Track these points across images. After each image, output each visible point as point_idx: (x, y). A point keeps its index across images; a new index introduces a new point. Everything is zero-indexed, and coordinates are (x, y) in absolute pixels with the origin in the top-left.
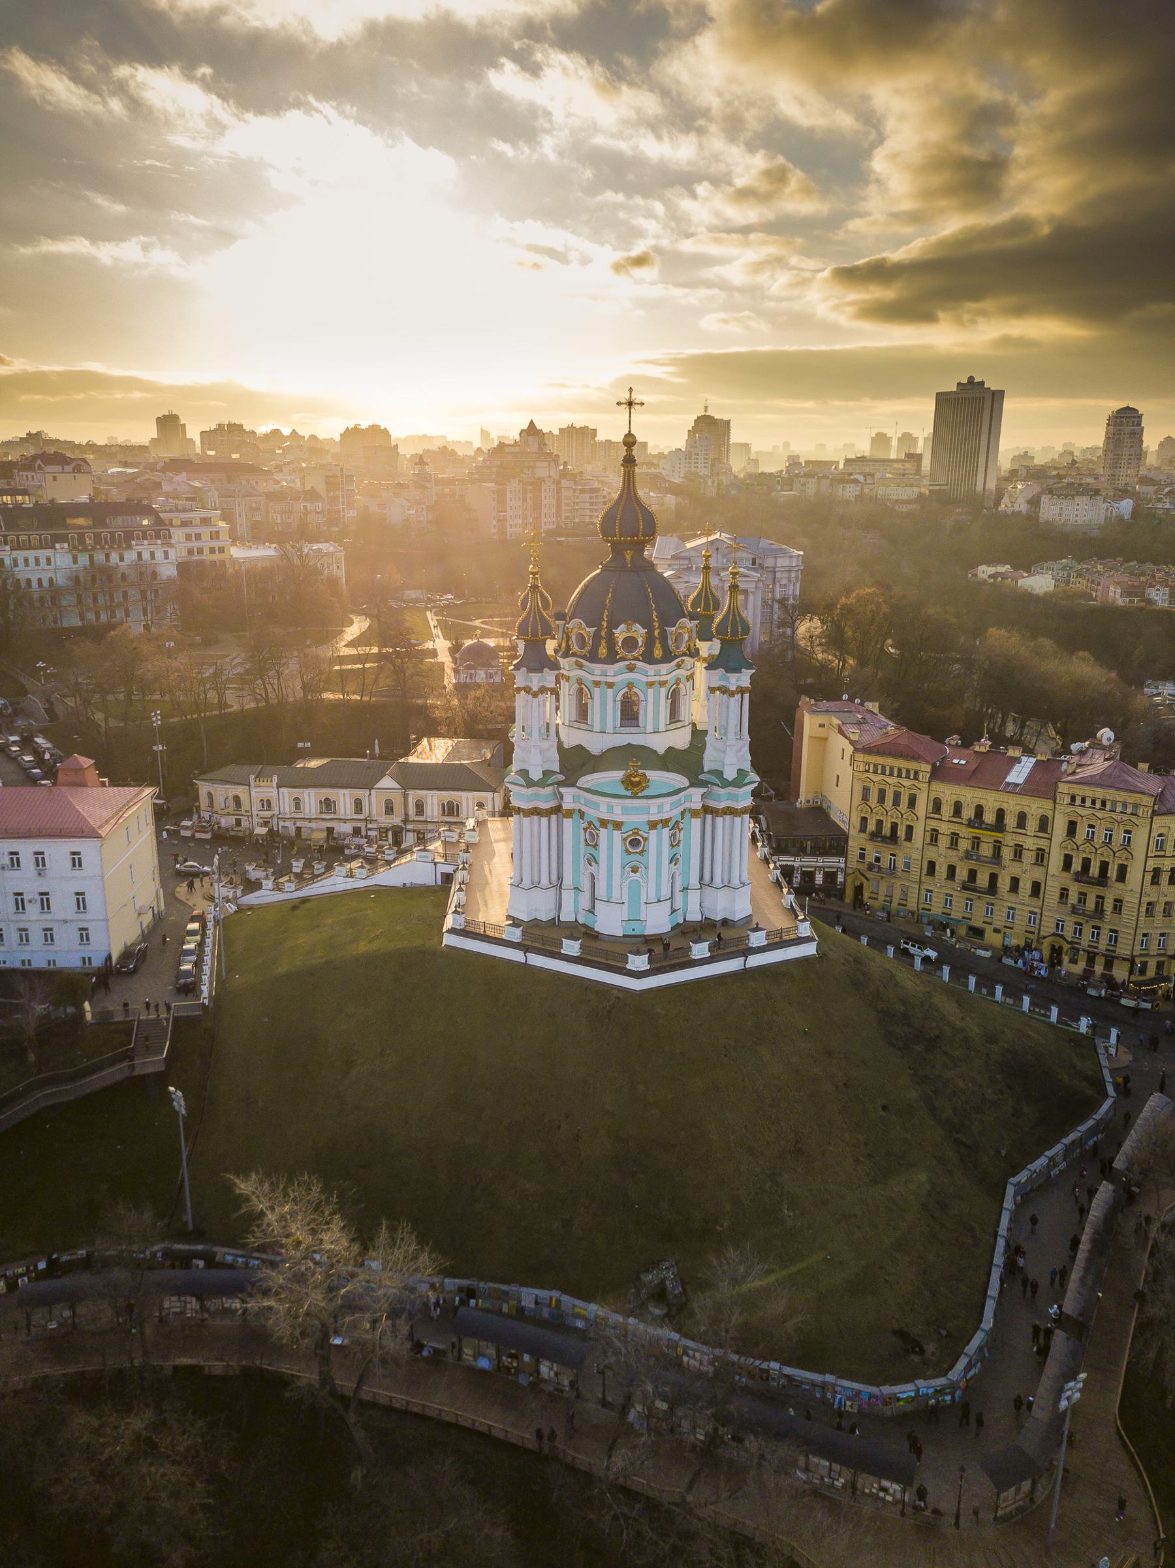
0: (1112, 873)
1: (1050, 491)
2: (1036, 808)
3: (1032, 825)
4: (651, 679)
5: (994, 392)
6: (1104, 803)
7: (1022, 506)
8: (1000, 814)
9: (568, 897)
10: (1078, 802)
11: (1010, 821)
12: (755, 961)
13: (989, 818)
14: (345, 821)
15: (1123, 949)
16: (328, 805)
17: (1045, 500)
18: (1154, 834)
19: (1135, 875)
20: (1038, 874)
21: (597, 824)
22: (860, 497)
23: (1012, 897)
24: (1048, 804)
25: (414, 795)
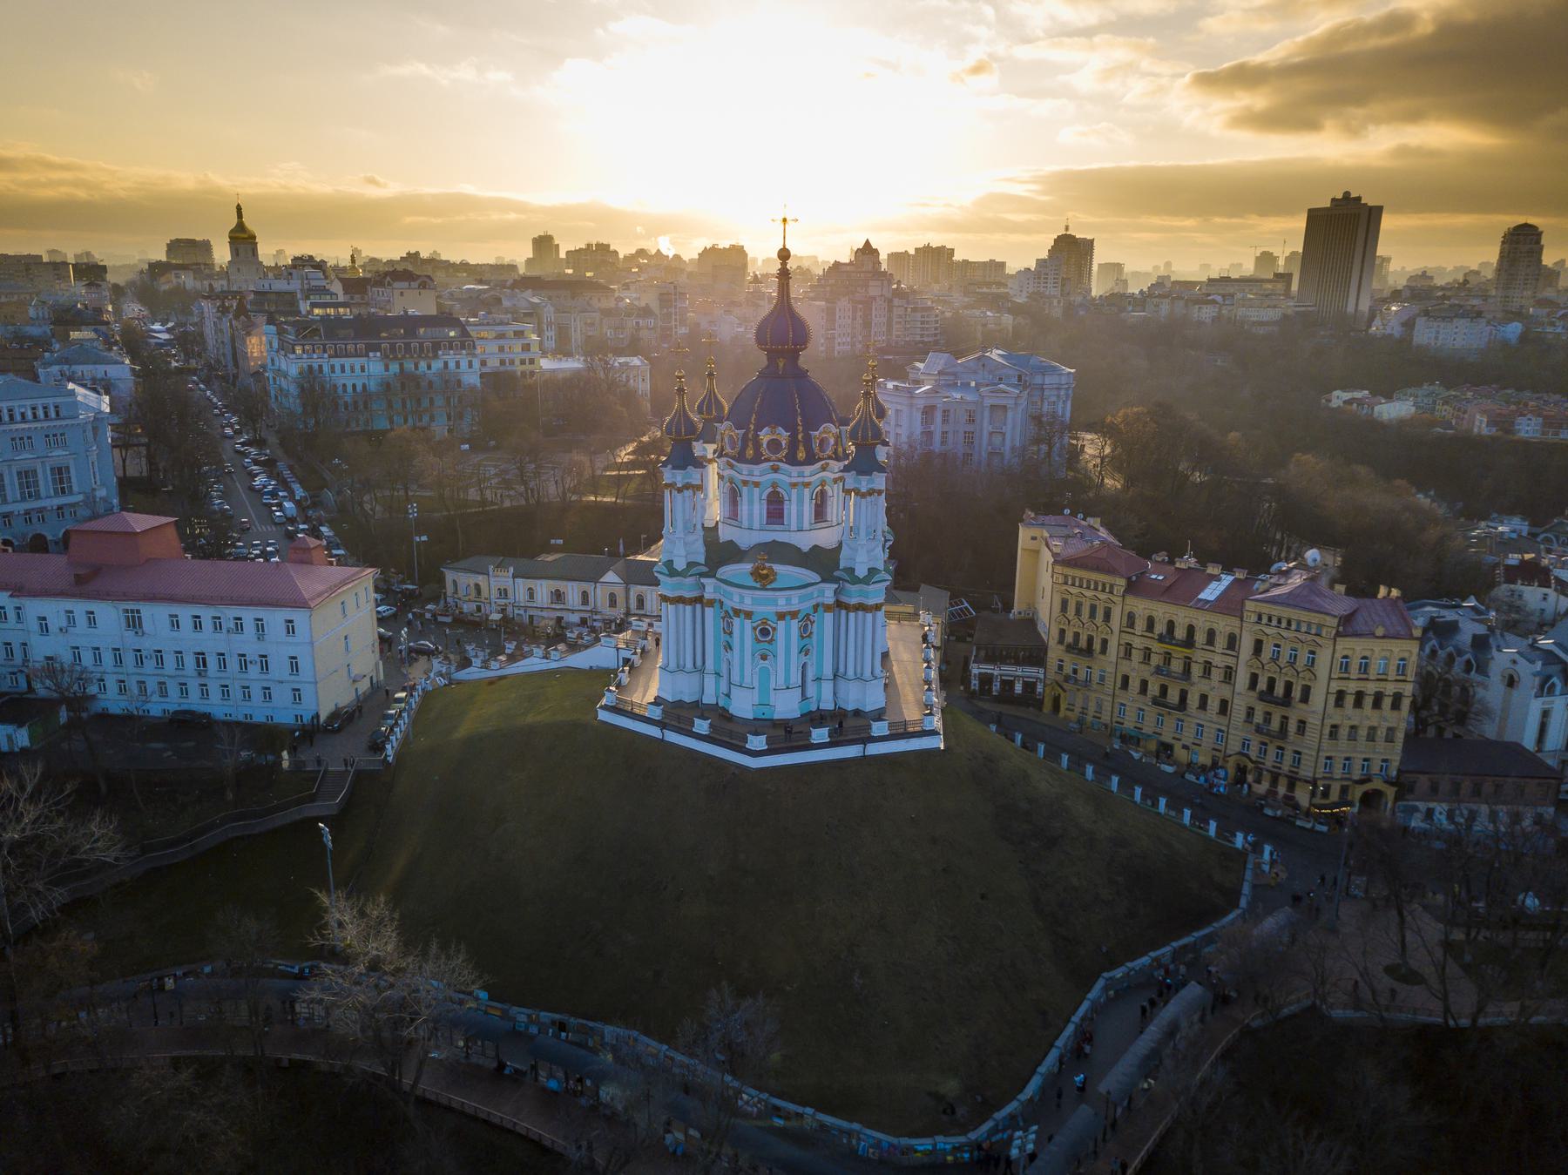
0: (1297, 693)
1: (1426, 313)
2: (1224, 625)
3: (1221, 642)
4: (794, 480)
5: (1371, 208)
7: (1396, 330)
8: (1191, 630)
9: (710, 681)
10: (1265, 620)
11: (1200, 638)
12: (874, 749)
13: (1180, 633)
14: (573, 611)
15: (1306, 771)
16: (558, 596)
17: (1421, 322)
18: (1338, 655)
19: (1318, 697)
20: (1225, 692)
22: (1216, 319)
23: (1201, 714)
24: (1236, 622)
25: (635, 590)
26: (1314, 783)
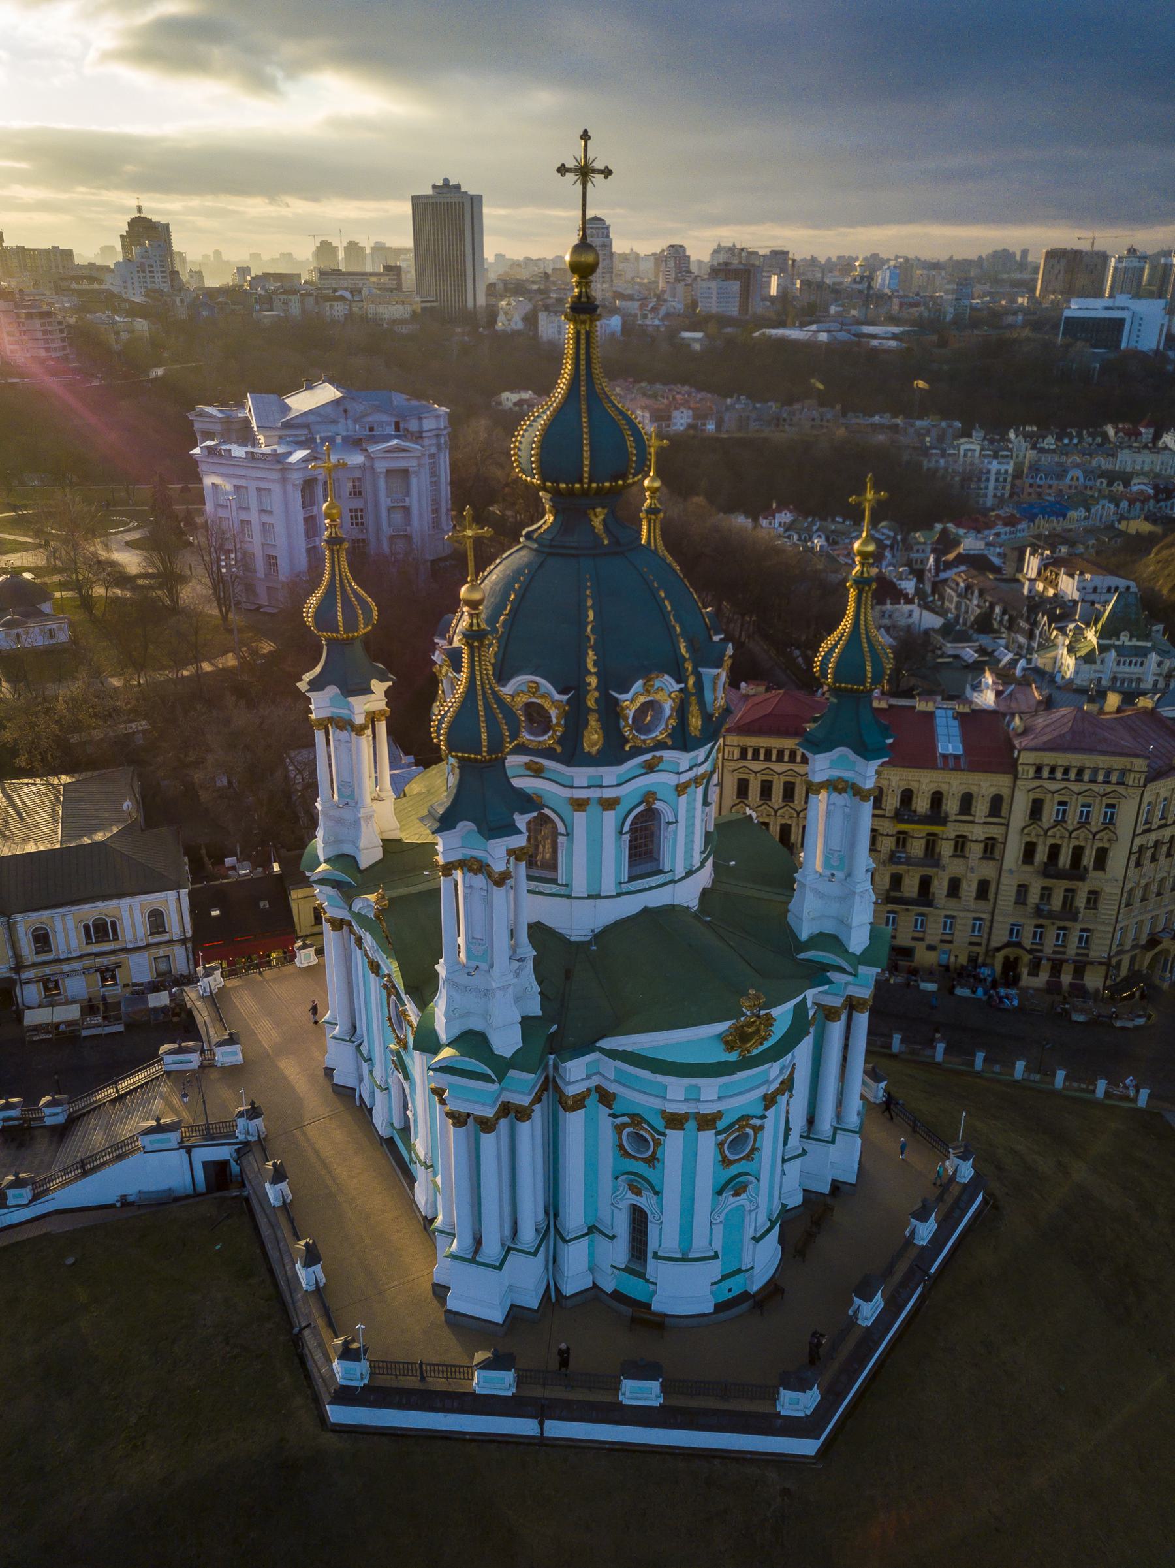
0: (1088, 859)
1: (547, 308)
2: (986, 785)
3: (981, 809)
5: (472, 197)
6: (1080, 772)
7: (518, 324)
8: (937, 799)
10: (1045, 773)
11: (951, 806)
13: (922, 805)
15: (1099, 951)
17: (542, 317)
18: (1144, 805)
19: (1118, 860)
20: (987, 870)
21: (659, 1124)
22: (350, 316)
23: (953, 903)
26: (1108, 964)
